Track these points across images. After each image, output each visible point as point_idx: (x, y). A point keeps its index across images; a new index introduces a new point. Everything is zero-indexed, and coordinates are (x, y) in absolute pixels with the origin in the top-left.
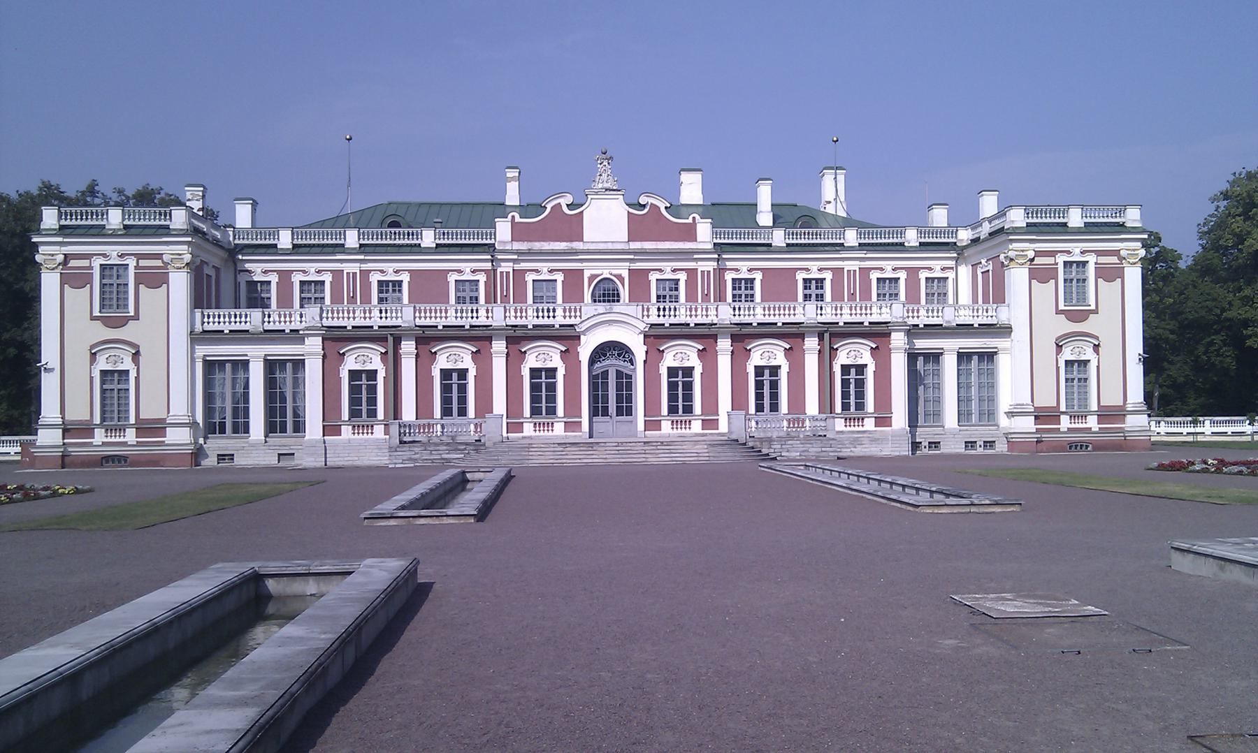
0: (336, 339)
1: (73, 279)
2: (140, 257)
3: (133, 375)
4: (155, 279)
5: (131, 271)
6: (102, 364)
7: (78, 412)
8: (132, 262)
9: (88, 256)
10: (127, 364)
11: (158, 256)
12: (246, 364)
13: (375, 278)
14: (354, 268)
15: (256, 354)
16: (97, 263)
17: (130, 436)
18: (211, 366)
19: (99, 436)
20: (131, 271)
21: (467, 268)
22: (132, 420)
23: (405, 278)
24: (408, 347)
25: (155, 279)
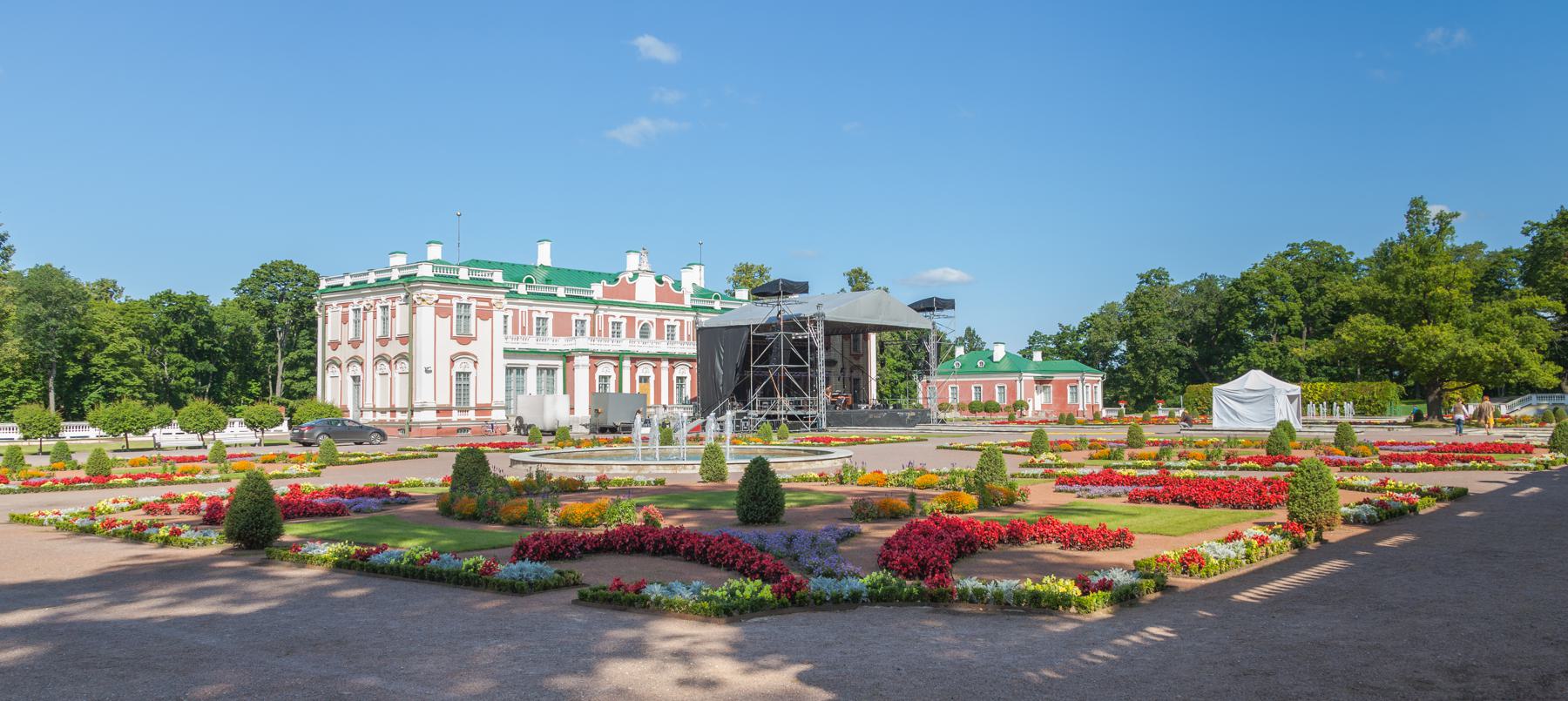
0: (596, 357)
1: (442, 312)
2: (479, 299)
3: (472, 377)
4: (485, 315)
5: (473, 310)
6: (458, 367)
7: (444, 400)
8: (474, 303)
9: (450, 297)
10: (470, 368)
11: (489, 300)
12: (521, 370)
13: (535, 315)
14: (525, 308)
15: (533, 364)
16: (455, 301)
17: (472, 415)
18: (509, 370)
19: (456, 415)
20: (473, 310)
21: (581, 312)
22: (472, 404)
23: (551, 316)
24: (627, 363)
25: (485, 315)
